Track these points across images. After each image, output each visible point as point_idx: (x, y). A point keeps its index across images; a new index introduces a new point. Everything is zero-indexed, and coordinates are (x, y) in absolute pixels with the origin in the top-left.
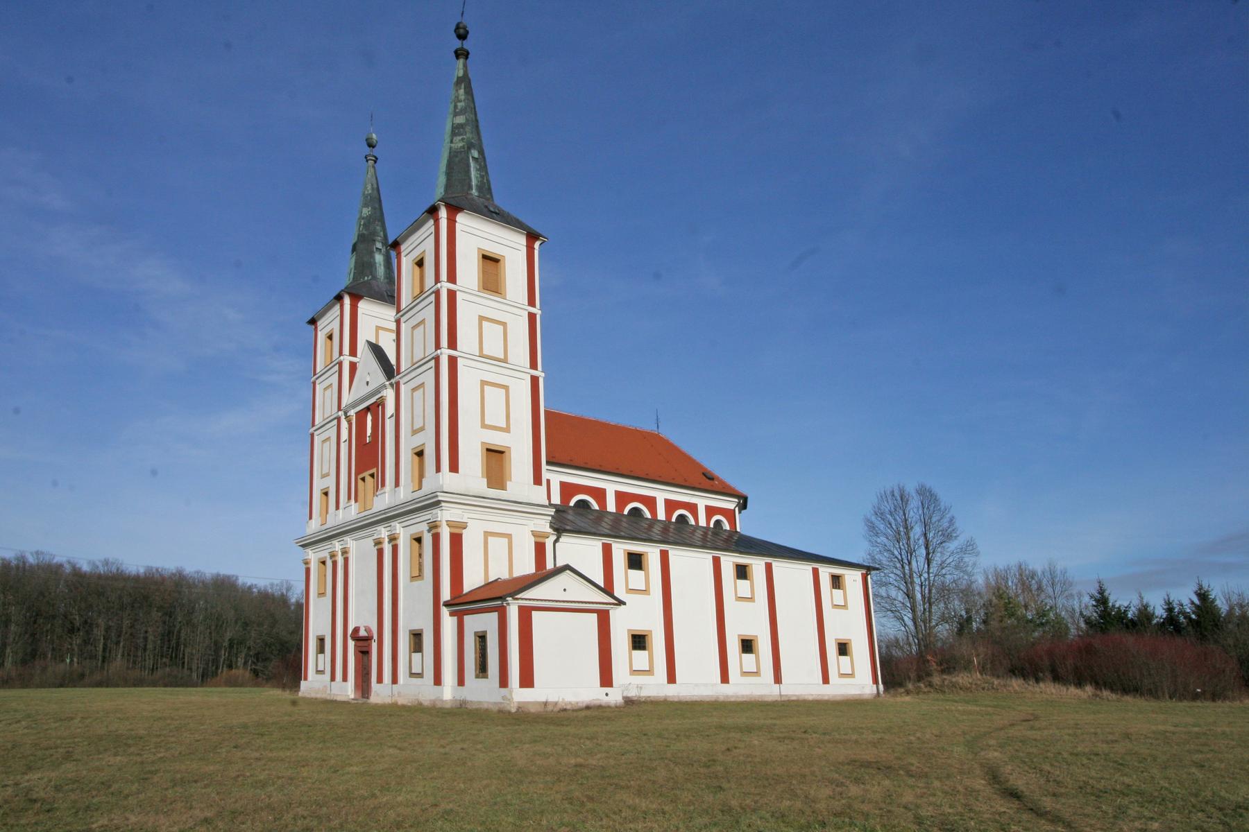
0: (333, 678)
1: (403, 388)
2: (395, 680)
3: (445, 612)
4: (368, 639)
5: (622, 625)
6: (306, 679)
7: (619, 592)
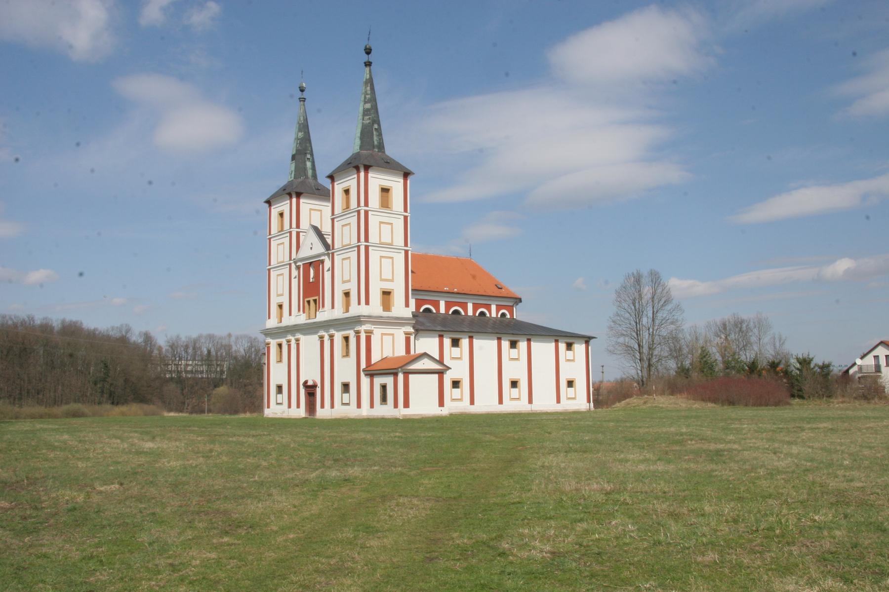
1: (336, 257)
2: (332, 406)
3: (362, 374)
4: (314, 386)
5: (448, 378)
6: (268, 407)
7: (447, 362)
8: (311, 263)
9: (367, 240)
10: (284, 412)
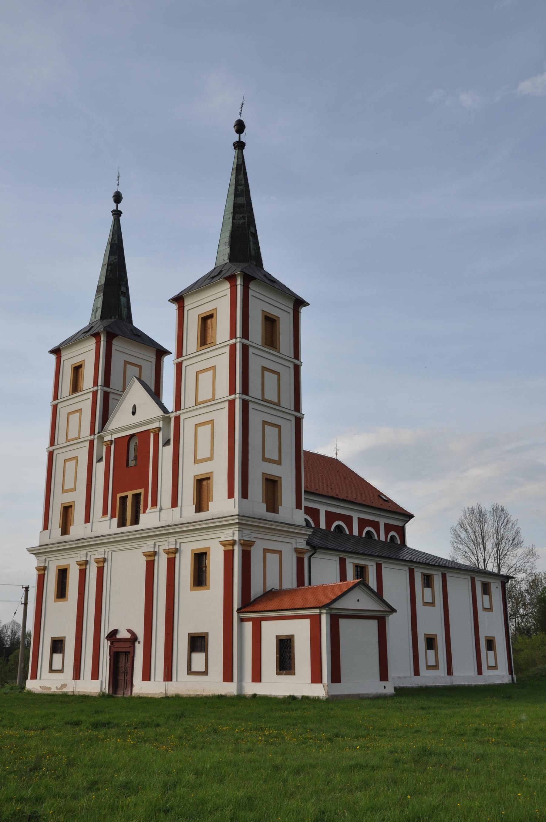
0: (77, 675)
2: (168, 676)
6: (34, 677)
8: (132, 436)
9: (245, 390)
10: (64, 686)
